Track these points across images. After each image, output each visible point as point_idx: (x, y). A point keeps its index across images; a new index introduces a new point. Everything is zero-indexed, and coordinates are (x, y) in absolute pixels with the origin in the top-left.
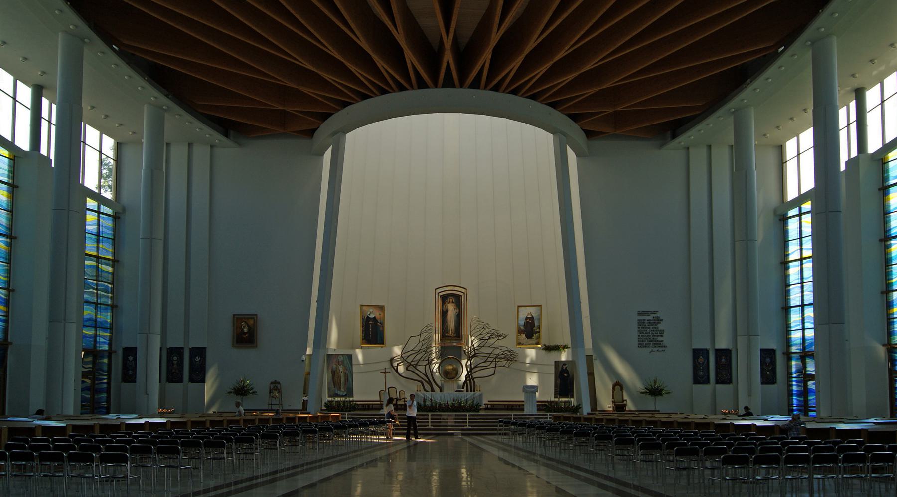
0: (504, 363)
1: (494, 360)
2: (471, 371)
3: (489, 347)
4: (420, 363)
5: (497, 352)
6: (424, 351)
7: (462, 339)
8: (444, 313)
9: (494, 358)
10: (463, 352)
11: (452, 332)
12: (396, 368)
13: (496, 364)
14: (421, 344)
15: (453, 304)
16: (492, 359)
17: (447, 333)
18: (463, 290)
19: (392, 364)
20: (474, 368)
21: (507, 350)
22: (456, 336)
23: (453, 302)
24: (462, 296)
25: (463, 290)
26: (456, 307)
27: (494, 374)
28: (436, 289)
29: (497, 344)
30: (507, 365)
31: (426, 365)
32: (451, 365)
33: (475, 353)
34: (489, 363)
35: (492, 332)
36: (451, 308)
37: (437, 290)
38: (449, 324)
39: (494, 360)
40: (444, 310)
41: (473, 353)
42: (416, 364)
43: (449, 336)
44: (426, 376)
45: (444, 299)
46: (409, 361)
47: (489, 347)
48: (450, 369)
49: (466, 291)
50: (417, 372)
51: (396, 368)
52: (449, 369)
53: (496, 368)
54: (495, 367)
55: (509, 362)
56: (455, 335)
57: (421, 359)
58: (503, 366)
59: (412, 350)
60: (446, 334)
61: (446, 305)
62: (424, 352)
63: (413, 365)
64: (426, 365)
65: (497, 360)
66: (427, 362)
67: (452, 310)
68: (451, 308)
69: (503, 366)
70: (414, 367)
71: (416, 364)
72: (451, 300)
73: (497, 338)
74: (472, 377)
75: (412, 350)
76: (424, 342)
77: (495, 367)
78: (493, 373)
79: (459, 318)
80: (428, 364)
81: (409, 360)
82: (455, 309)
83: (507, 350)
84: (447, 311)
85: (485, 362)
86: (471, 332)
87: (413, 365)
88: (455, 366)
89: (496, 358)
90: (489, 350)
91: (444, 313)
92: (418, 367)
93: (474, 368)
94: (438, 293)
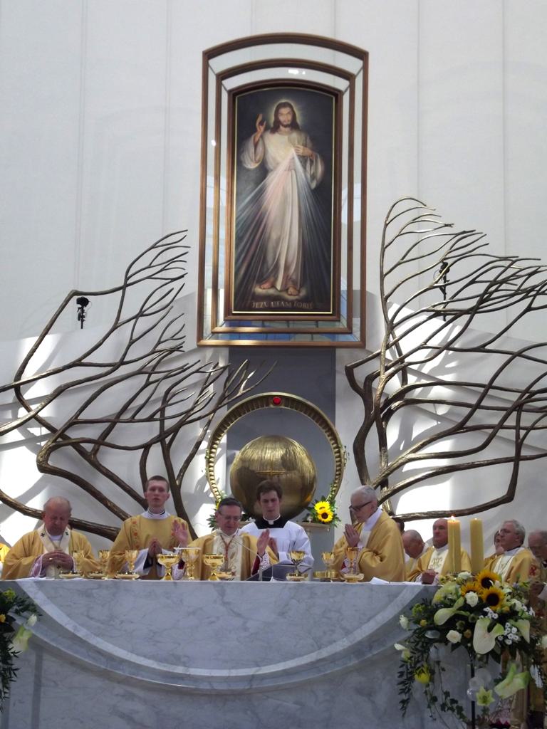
1: (511, 421)
4: (122, 434)
5: (521, 375)
6: (140, 372)
7: (337, 312)
9: (509, 412)
10: (341, 380)
11: (286, 277)
13: (519, 445)
14: (125, 332)
15: (295, 135)
17: (261, 281)
18: (350, 64)
22: (305, 300)
23: (293, 126)
24: (337, 94)
25: (350, 64)
26: (308, 152)
28: (210, 54)
31: (147, 447)
35: (490, 276)
37: (211, 62)
38: (274, 236)
39: (511, 421)
41: (395, 385)
47: (481, 349)
49: (365, 69)
50: (103, 485)
52: (262, 463)
53: (522, 463)
54: (517, 459)
56: (303, 293)
57: (127, 416)
59: (78, 363)
60: (259, 290)
61: (258, 135)
64: (147, 447)
65: (527, 419)
66: (153, 429)
67: (291, 168)
70: (82, 452)
72: (285, 115)
73: (527, 302)
75: (78, 363)
76: (143, 324)
77: (517, 459)
78: (502, 492)
80: (160, 439)
82: (303, 159)
86: (382, 277)
87: (76, 445)
89: (518, 407)
90: (482, 370)
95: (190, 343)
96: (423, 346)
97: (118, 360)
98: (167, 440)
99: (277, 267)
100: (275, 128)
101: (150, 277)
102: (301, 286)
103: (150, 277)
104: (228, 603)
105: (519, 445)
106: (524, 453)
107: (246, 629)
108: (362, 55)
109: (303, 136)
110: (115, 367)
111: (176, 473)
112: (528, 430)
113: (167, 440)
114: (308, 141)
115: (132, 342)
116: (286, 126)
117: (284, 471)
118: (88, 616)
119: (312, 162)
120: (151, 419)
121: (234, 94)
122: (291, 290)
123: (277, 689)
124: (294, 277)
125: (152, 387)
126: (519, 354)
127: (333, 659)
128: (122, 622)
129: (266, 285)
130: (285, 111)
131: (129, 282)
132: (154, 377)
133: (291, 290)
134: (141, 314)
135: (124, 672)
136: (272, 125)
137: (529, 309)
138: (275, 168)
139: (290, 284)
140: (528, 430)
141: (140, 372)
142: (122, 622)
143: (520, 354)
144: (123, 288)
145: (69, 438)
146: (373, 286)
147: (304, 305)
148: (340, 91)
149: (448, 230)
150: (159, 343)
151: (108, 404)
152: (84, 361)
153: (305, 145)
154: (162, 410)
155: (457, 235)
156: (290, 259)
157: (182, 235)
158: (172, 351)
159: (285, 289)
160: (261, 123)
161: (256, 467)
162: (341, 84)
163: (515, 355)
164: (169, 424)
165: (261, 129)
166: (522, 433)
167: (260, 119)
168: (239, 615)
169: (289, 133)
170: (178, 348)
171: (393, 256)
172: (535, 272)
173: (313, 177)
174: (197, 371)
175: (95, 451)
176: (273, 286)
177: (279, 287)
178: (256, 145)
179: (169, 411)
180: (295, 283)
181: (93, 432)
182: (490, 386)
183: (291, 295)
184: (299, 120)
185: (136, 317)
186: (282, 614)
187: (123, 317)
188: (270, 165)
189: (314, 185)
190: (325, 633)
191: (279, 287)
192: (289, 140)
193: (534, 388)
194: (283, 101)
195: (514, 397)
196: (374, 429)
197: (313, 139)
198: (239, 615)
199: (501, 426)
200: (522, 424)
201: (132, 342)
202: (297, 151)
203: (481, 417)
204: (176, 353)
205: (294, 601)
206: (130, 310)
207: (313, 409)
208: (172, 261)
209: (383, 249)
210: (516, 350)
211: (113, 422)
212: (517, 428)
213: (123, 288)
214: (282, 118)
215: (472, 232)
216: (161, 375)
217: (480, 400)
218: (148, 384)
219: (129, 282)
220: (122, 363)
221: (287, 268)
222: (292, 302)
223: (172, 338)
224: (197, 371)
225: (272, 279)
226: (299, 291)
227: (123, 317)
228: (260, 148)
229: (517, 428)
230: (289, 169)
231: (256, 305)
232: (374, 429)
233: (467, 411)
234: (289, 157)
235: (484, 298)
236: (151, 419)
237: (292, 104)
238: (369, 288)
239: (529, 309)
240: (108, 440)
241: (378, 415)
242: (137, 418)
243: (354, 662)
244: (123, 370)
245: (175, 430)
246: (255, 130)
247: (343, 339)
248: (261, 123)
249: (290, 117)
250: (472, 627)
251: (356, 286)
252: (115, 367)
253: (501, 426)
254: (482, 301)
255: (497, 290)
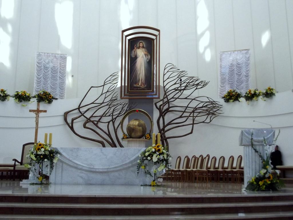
0: (203, 118)
1: (192, 115)
2: (163, 129)
3: (186, 98)
5: (194, 104)
6: (107, 105)
8: (132, 60)
9: (191, 113)
11: (141, 82)
12: (71, 125)
13: (194, 120)
14: (104, 96)
15: (143, 49)
16: (188, 114)
17: (136, 83)
18: (156, 33)
19: (65, 120)
20: (169, 124)
21: (209, 102)
22: (146, 87)
23: (143, 47)
24: (153, 40)
25: (156, 33)
27: (191, 133)
29: (195, 95)
30: (208, 120)
32: (136, 120)
33: (169, 107)
34: (184, 119)
35: (187, 81)
36: (141, 54)
38: (139, 73)
39: (192, 115)
40: (133, 56)
41: (166, 107)
42: (99, 121)
43: (137, 87)
44: (109, 135)
45: (133, 43)
46: (88, 117)
47: (186, 98)
48: (135, 126)
49: (159, 34)
51: (71, 125)
53: (194, 125)
54: (193, 124)
55: (210, 115)
56: (145, 86)
57: (104, 115)
58: (203, 122)
59: (93, 103)
60: (135, 85)
62: (108, 107)
63: (93, 122)
64: (109, 122)
65: (195, 114)
66: (110, 118)
67: (143, 57)
68: (141, 54)
69: (203, 122)
70: (94, 124)
71: (99, 121)
72: (141, 45)
74: (165, 136)
75: (93, 103)
76: (108, 94)
77: (193, 124)
78: (190, 131)
79: (150, 64)
80: (112, 120)
81: (88, 115)
82: (145, 55)
83: (209, 102)
84: (136, 57)
85: (181, 117)
86: (164, 82)
87: (93, 122)
88: (142, 122)
89: (193, 112)
90: (185, 103)
91: (132, 60)
92: (100, 125)
93: (169, 124)
94: (126, 36)
95: (119, 98)
96: (173, 98)
97: (102, 102)
98: (114, 120)
99: (139, 80)
100: (139, 48)
101: (110, 83)
102: (145, 84)
103: (110, 83)
104: (103, 152)
105: (194, 120)
106: (195, 122)
107: (106, 158)
108: (158, 31)
109: (145, 49)
110: (101, 104)
111: (116, 128)
112: (196, 117)
113: (114, 120)
114: (147, 51)
115: (105, 98)
116: (141, 47)
117: (138, 127)
118: (72, 155)
119: (147, 55)
120: (109, 116)
121: (129, 40)
122: (143, 85)
123: (113, 171)
124: (143, 82)
125: (110, 109)
126: (194, 99)
127: (126, 164)
128: (79, 157)
129: (137, 84)
130: (141, 44)
131: (105, 84)
132: (110, 106)
133: (143, 85)
134: (108, 91)
135: (80, 167)
136: (138, 47)
137: (196, 89)
138: (139, 57)
139: (142, 84)
140: (196, 117)
141: (107, 105)
142: (79, 157)
143: (194, 99)
144: (103, 86)
145: (91, 120)
146: (161, 84)
147: (146, 89)
148: (154, 39)
149: (179, 71)
150: (112, 98)
151: (100, 113)
152: (94, 102)
153: (146, 52)
154: (112, 113)
155: (181, 72)
156: (142, 78)
157: (117, 73)
158: (115, 100)
159: (141, 85)
160: (136, 47)
161: (132, 126)
162: (154, 37)
163: (193, 100)
164: (114, 117)
165: (135, 48)
166: (194, 118)
167: (135, 46)
168: (105, 155)
169: (142, 49)
170: (116, 99)
171: (166, 77)
172: (197, 80)
173: (148, 59)
174: (120, 105)
175: (97, 123)
176: (138, 85)
177: (140, 84)
178: (134, 52)
179: (114, 114)
180: (143, 84)
181: (97, 119)
182: (187, 107)
183: (143, 87)
184: (144, 46)
185: (106, 92)
186: (115, 155)
187: (103, 93)
188: (138, 56)
189: (148, 61)
190: (124, 159)
191: (140, 85)
192: (142, 51)
193: (197, 107)
194: (141, 41)
195: (192, 109)
196: (161, 117)
197: (148, 50)
198: (105, 155)
199: (189, 116)
200: (194, 115)
201: (105, 98)
202: (144, 52)
203: (185, 114)
204: (116, 101)
205: (117, 152)
206: (105, 91)
207: (145, 113)
208: (115, 79)
209: (164, 75)
210: (193, 98)
211: (101, 117)
212: (193, 116)
213: (103, 86)
214: (140, 45)
215: (184, 71)
216: (112, 106)
217: (185, 110)
218: (109, 108)
219: (105, 84)
220: (103, 103)
221: (142, 80)
222: (143, 88)
223: (115, 97)
224: (120, 105)
225: (138, 83)
226: (144, 86)
227: (103, 93)
228: (135, 52)
229: (193, 116)
230: (142, 57)
231: (134, 89)
232: (161, 117)
233: (182, 113)
234: (142, 55)
235: (186, 86)
236: (109, 116)
237: (143, 42)
238: (160, 85)
239: (196, 89)
240: (100, 121)
241: (162, 114)
242: (106, 115)
243: (130, 165)
244: (103, 105)
245: (116, 118)
246: (134, 48)
247: (154, 96)
248: (136, 47)
249: (142, 45)
250: (152, 156)
251: (158, 84)
252: (101, 104)
253: (189, 116)
254: (186, 87)
255: (189, 85)
